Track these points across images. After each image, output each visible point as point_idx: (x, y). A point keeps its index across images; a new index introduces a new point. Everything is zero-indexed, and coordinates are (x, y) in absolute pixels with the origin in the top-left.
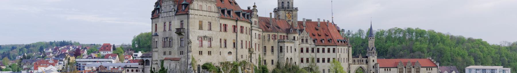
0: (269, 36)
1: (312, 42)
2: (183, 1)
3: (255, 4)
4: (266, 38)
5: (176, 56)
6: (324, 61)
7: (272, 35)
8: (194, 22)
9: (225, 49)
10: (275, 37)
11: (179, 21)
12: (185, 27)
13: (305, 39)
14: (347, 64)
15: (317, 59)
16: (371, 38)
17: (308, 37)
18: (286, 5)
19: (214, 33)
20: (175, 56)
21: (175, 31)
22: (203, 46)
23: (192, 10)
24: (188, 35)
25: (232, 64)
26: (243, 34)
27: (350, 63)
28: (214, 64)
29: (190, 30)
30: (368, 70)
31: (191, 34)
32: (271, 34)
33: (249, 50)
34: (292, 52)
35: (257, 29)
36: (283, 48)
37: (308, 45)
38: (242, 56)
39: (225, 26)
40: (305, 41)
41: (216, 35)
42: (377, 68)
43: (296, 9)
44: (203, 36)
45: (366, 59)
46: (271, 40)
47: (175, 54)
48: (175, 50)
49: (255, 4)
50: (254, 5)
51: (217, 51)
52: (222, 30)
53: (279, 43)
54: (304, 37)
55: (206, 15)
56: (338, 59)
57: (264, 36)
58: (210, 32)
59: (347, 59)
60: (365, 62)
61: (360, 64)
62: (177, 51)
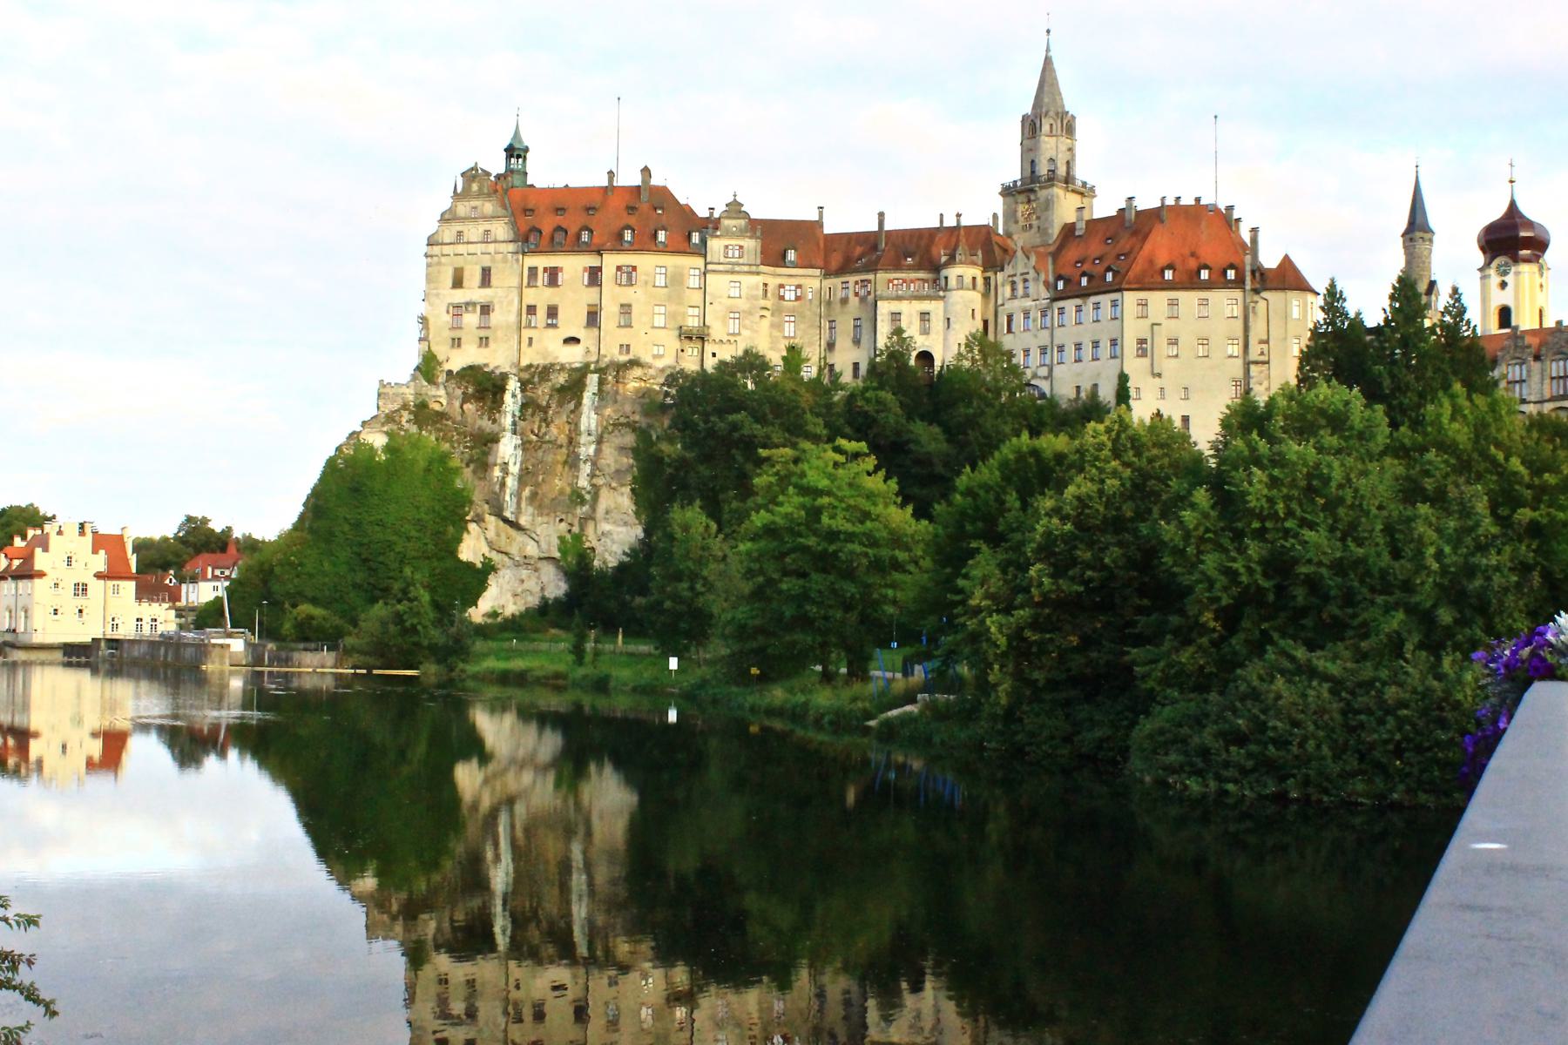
3: (735, 196)
4: (834, 295)
8: (439, 272)
9: (551, 331)
13: (1018, 279)
17: (1028, 273)
19: (499, 290)
28: (497, 367)
32: (852, 279)
35: (754, 269)
37: (1028, 303)
44: (463, 300)
49: (735, 196)
50: (731, 199)
54: (1015, 275)
58: (487, 291)
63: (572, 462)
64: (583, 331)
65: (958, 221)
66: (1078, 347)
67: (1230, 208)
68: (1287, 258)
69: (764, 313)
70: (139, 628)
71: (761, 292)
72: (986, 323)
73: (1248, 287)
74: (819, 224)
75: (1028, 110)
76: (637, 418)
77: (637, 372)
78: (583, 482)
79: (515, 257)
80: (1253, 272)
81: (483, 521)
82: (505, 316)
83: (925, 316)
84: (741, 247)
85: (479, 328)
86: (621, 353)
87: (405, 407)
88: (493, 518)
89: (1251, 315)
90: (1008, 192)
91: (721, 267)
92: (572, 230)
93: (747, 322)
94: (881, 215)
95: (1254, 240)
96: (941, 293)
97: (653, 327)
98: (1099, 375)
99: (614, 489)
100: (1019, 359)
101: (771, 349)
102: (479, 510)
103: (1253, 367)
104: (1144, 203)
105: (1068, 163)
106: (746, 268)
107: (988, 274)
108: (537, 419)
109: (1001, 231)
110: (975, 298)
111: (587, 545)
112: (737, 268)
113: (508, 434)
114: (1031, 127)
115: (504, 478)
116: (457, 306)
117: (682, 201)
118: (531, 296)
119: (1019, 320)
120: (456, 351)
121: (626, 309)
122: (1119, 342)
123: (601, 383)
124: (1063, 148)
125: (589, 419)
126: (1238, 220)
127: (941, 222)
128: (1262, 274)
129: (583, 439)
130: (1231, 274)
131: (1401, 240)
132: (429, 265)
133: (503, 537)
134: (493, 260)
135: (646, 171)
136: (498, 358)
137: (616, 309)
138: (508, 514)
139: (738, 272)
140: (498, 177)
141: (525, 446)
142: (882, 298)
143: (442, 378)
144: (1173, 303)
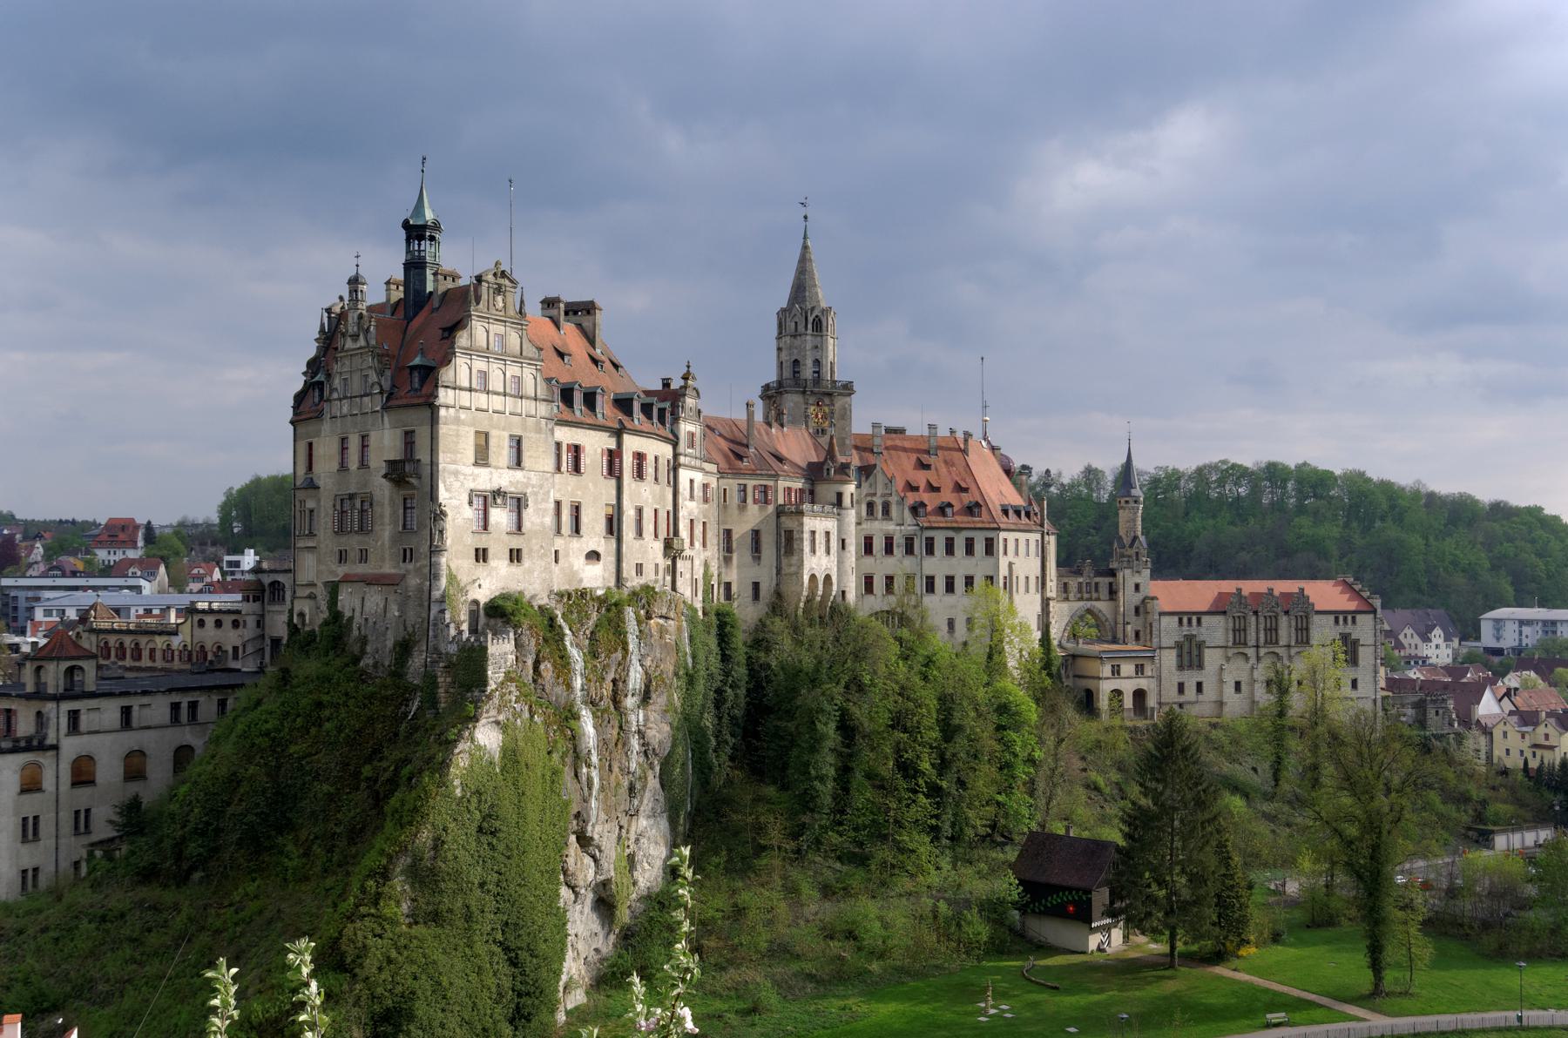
0: (744, 490)
1: (907, 513)
2: (416, 356)
3: (688, 367)
4: (731, 497)
5: (388, 569)
6: (950, 586)
7: (755, 487)
8: (458, 435)
9: (575, 544)
10: (765, 493)
11: (399, 433)
12: (422, 455)
13: (878, 501)
14: (1038, 596)
15: (927, 577)
16: (1127, 502)
18: (808, 372)
20: (381, 567)
21: (383, 472)
22: (490, 528)
23: (449, 390)
24: (432, 486)
25: (602, 601)
26: (643, 484)
27: (1049, 594)
28: (533, 597)
29: (440, 467)
30: (1116, 623)
31: (444, 482)
32: (751, 483)
33: (668, 545)
34: (832, 551)
35: (698, 463)
36: (796, 535)
38: (639, 569)
39: (576, 450)
41: (541, 486)
42: (1150, 617)
43: (848, 389)
44: (488, 488)
45: (1111, 579)
47: (383, 559)
48: (383, 544)
49: (688, 367)
51: (542, 546)
52: (564, 468)
53: (783, 519)
54: (875, 494)
55: (500, 408)
56: (1005, 578)
57: (725, 490)
59: (1037, 582)
60: (1104, 592)
61: (1088, 600)
62: (390, 548)
64: (603, 540)
119: (878, 544)
134: (525, 428)
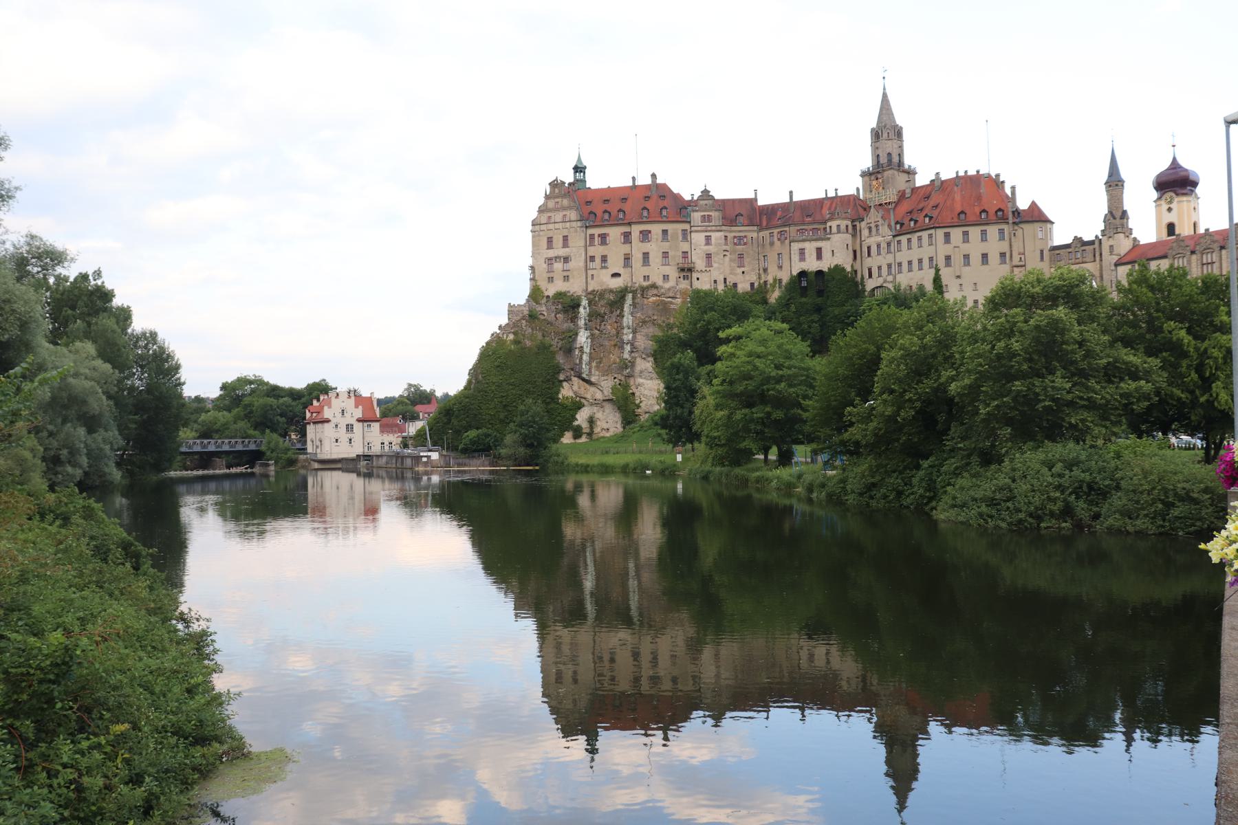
7: (778, 233)
9: (604, 271)
28: (575, 293)
32: (776, 231)
35: (718, 228)
37: (879, 239)
40: (874, 230)
44: (553, 256)
46: (777, 243)
58: (567, 249)
63: (620, 345)
65: (836, 193)
66: (910, 263)
67: (998, 176)
68: (1034, 205)
69: (726, 253)
70: (382, 448)
71: (723, 241)
72: (855, 252)
73: (1011, 222)
74: (756, 200)
75: (874, 125)
76: (655, 318)
77: (655, 292)
78: (626, 356)
79: (582, 229)
80: (1013, 212)
81: (570, 380)
82: (577, 263)
83: (819, 251)
84: (711, 216)
85: (564, 271)
86: (644, 280)
87: (523, 318)
88: (576, 379)
89: (1013, 237)
90: (864, 174)
91: (699, 228)
92: (614, 213)
93: (716, 259)
94: (791, 192)
95: (1013, 193)
96: (828, 236)
97: (663, 265)
98: (923, 278)
99: (644, 359)
100: (875, 272)
101: (731, 274)
102: (568, 374)
103: (1015, 269)
104: (944, 177)
105: (899, 155)
106: (714, 228)
107: (855, 223)
108: (598, 321)
109: (861, 197)
110: (848, 237)
111: (631, 391)
112: (709, 228)
113: (583, 330)
114: (876, 135)
115: (581, 356)
116: (550, 259)
117: (675, 191)
118: (592, 251)
120: (550, 284)
121: (646, 256)
122: (934, 258)
123: (634, 298)
124: (895, 146)
125: (628, 320)
126: (1003, 182)
127: (826, 194)
128: (1019, 213)
129: (625, 331)
130: (1000, 213)
131: (1104, 186)
132: (533, 237)
133: (582, 389)
135: (654, 176)
136: (575, 287)
137: (641, 256)
138: (584, 376)
139: (710, 231)
140: (570, 184)
141: (592, 337)
142: (794, 241)
143: (544, 300)
144: (966, 234)
